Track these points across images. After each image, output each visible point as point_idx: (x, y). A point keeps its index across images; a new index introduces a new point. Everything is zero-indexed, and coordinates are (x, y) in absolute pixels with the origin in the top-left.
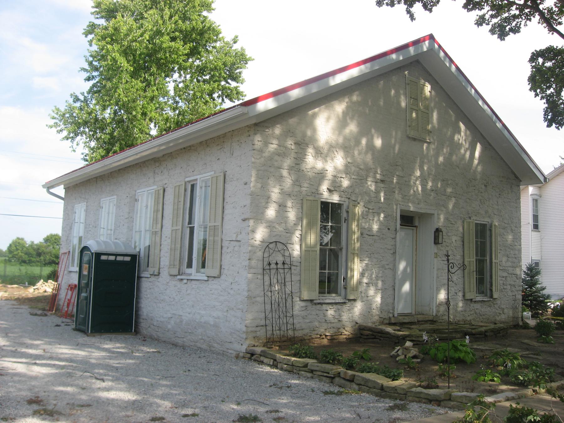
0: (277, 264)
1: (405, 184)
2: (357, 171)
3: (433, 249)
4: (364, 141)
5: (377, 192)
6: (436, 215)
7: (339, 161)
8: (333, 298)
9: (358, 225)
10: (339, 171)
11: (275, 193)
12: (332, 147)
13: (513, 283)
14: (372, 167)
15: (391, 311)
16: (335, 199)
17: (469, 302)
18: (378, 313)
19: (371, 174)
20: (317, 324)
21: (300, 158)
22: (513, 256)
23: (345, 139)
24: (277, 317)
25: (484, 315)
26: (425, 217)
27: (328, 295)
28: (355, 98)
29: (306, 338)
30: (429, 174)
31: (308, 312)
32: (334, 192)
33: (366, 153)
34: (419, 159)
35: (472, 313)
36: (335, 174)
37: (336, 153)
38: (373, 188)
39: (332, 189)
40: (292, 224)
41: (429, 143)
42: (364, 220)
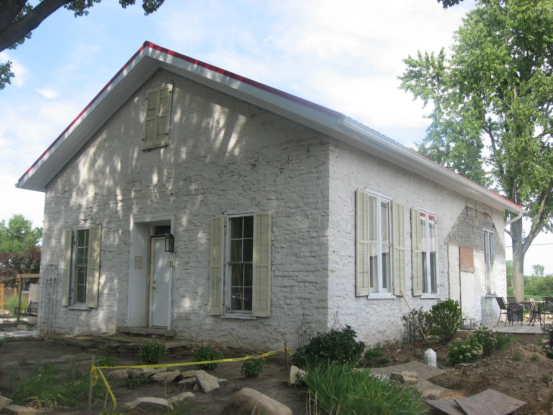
0: (51, 280)
8: (83, 307)
13: (307, 296)
22: (308, 254)
25: (244, 339)
41: (166, 146)
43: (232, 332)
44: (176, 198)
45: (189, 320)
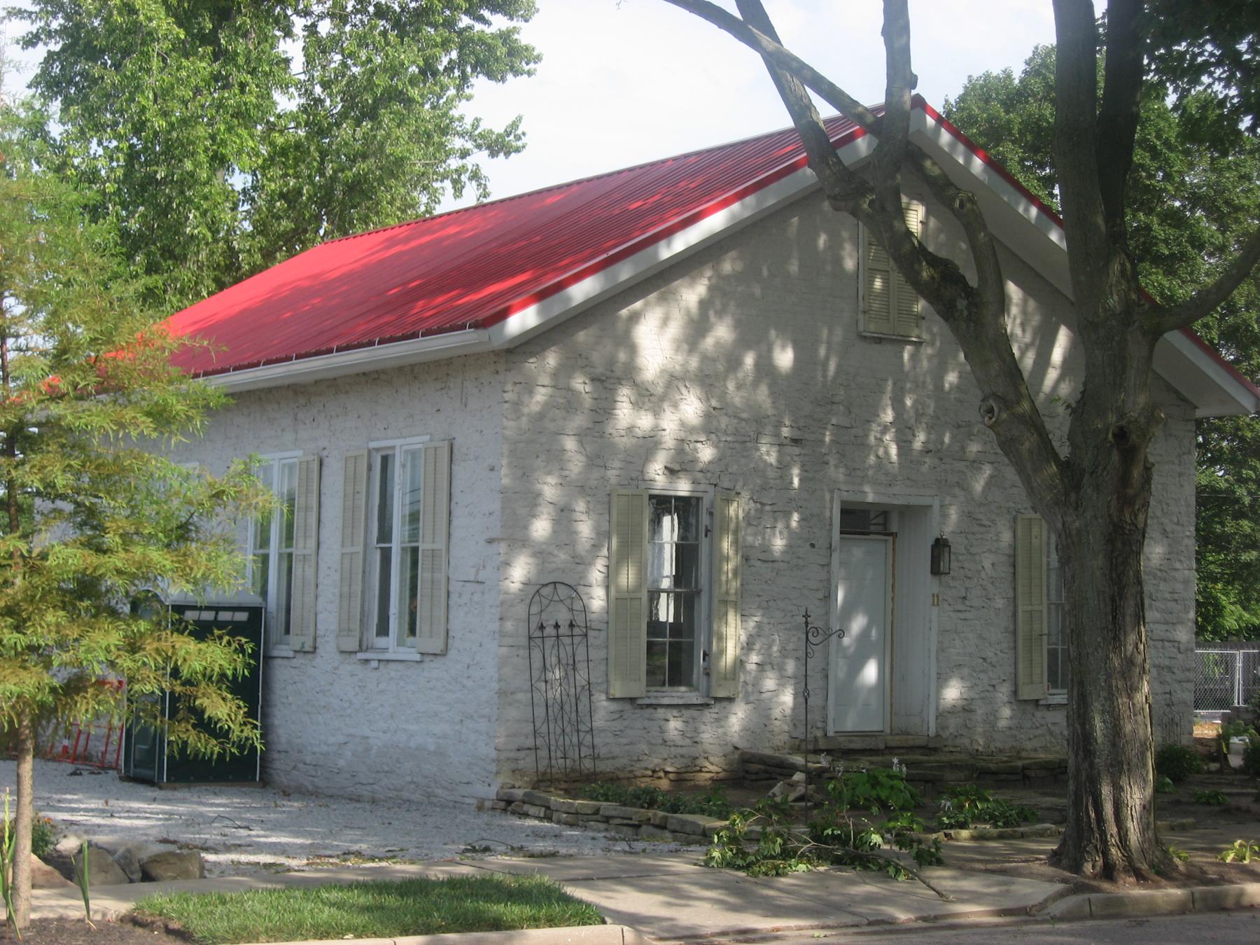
0: (557, 626)
1: (853, 443)
2: (733, 429)
3: (929, 585)
4: (749, 360)
5: (783, 467)
6: (936, 504)
7: (691, 407)
8: (681, 694)
9: (736, 542)
10: (692, 430)
11: (549, 488)
12: (673, 381)
13: (1167, 662)
14: (770, 412)
15: (820, 725)
16: (683, 488)
17: (1030, 708)
18: (786, 728)
19: (769, 429)
20: (644, 747)
21: (604, 410)
22: (1168, 596)
23: (705, 358)
24: (559, 731)
26: (911, 513)
27: (671, 689)
28: (727, 267)
29: (621, 775)
30: (919, 416)
31: (626, 723)
32: (681, 475)
33: (756, 383)
34: (890, 383)
35: (1039, 732)
36: (683, 435)
37: (684, 390)
38: (772, 458)
39: (677, 467)
40: (587, 546)
41: (918, 345)
42: (750, 530)
43: (1053, 728)
44: (937, 461)
45: (971, 711)
